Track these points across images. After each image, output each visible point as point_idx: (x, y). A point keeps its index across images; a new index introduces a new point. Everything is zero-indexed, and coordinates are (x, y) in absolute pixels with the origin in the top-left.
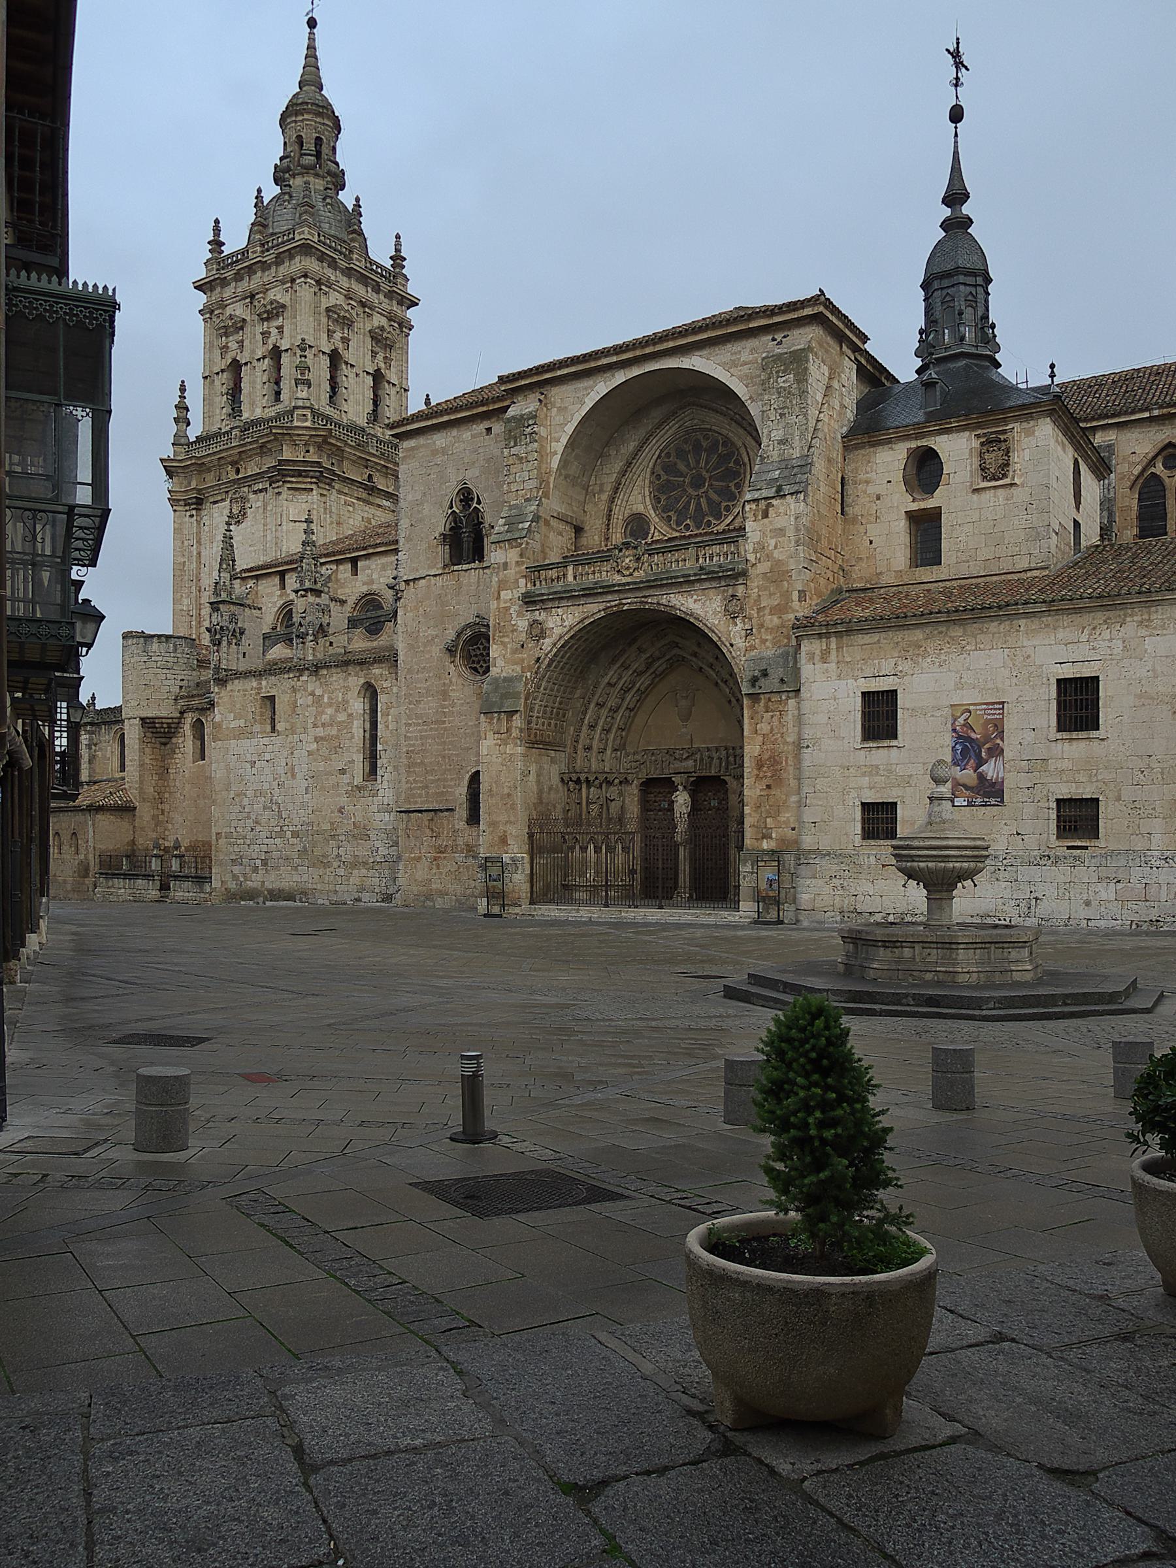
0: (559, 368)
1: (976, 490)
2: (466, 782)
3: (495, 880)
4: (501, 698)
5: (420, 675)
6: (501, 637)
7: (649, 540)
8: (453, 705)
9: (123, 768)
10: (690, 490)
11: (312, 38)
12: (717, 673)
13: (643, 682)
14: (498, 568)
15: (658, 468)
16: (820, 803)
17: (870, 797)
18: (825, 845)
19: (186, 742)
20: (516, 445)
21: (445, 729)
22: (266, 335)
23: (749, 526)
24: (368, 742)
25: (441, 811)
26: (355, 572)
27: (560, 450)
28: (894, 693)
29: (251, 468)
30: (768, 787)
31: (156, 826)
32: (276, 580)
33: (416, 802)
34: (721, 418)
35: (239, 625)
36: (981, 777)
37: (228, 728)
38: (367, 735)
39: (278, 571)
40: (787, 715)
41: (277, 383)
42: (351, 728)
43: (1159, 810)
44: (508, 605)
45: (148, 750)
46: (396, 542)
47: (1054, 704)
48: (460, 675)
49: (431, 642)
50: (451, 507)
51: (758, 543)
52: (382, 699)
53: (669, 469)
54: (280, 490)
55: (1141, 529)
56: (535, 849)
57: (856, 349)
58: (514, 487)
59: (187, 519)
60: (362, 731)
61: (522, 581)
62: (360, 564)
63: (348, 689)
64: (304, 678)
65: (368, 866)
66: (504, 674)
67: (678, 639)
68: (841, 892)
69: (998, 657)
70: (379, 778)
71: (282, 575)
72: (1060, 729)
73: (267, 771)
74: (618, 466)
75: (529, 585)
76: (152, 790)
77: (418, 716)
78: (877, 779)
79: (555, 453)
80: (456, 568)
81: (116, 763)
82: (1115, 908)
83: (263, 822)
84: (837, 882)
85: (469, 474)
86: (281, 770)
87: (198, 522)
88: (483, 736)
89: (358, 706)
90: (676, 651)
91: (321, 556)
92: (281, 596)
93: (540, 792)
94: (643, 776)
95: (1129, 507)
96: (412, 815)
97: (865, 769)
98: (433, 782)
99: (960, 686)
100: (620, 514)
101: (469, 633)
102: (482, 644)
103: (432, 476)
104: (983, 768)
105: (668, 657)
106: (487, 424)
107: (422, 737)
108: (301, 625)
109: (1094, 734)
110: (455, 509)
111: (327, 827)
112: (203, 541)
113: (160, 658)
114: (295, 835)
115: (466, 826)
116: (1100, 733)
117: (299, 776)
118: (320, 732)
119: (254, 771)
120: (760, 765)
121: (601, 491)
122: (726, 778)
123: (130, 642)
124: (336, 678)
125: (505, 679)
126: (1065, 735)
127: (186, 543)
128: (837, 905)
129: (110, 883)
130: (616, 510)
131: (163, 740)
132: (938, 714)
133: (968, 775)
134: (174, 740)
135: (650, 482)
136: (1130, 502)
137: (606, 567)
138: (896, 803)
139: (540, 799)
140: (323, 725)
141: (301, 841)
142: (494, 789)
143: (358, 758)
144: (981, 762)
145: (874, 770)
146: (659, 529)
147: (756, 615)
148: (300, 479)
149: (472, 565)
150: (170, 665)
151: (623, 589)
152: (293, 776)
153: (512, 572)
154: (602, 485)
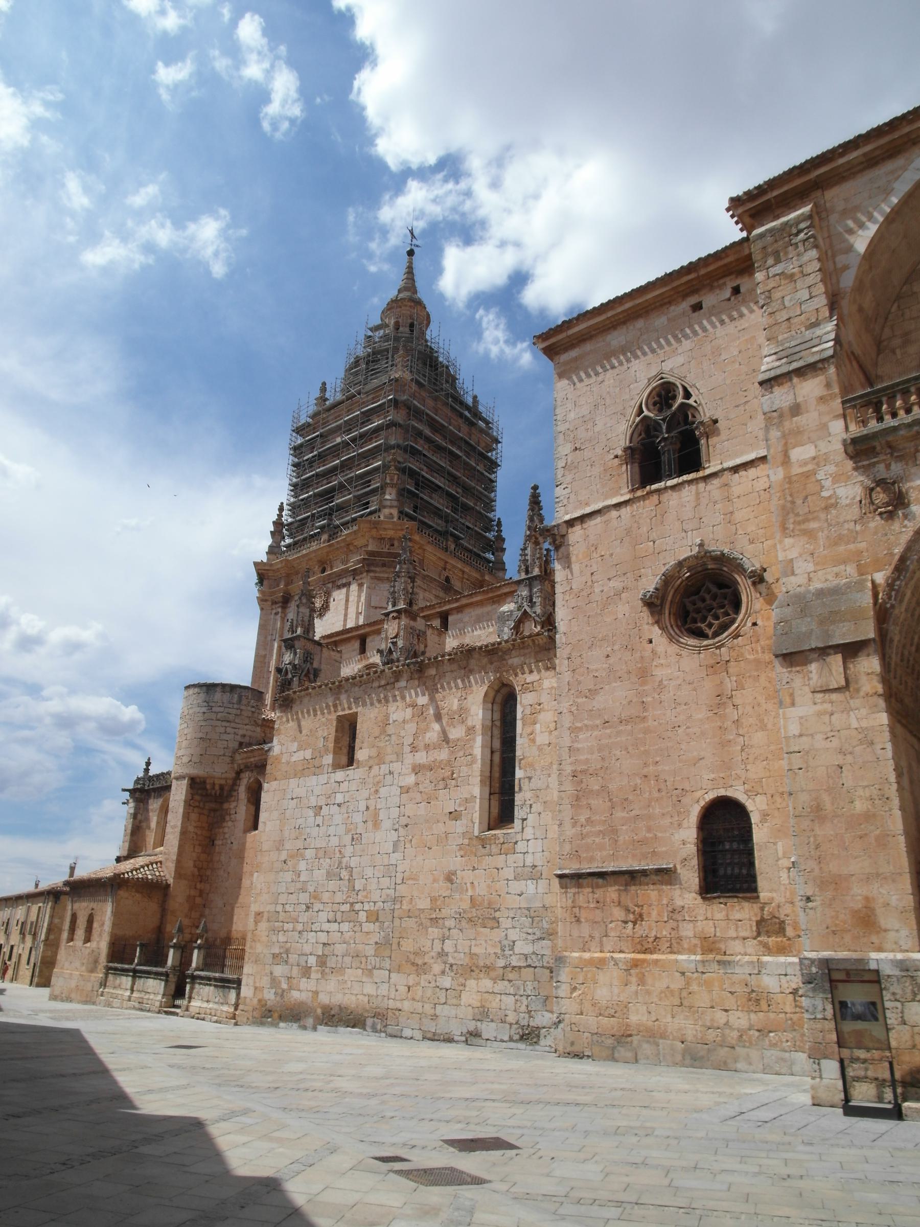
0: (842, 155)
3: (858, 1017)
4: (821, 623)
6: (799, 523)
8: (661, 686)
11: (411, 263)
14: (781, 416)
20: (778, 261)
21: (647, 731)
33: (592, 859)
35: (315, 665)
37: (288, 763)
38: (497, 758)
42: (472, 747)
44: (810, 467)
50: (641, 411)
58: (784, 315)
59: (272, 616)
61: (837, 426)
62: (450, 618)
64: (403, 683)
65: (493, 974)
66: (817, 585)
70: (517, 823)
73: (338, 819)
75: (853, 427)
79: (846, 268)
80: (654, 487)
83: (326, 897)
85: (667, 366)
86: (358, 818)
87: (283, 619)
88: (787, 700)
102: (709, 591)
103: (606, 383)
106: (693, 300)
110: (646, 413)
114: (374, 917)
115: (699, 900)
117: (387, 824)
118: (421, 757)
119: (319, 820)
125: (820, 593)
127: (269, 638)
140: (427, 747)
141: (381, 928)
142: (828, 806)
148: (384, 569)
149: (685, 477)
152: (377, 824)
153: (809, 419)
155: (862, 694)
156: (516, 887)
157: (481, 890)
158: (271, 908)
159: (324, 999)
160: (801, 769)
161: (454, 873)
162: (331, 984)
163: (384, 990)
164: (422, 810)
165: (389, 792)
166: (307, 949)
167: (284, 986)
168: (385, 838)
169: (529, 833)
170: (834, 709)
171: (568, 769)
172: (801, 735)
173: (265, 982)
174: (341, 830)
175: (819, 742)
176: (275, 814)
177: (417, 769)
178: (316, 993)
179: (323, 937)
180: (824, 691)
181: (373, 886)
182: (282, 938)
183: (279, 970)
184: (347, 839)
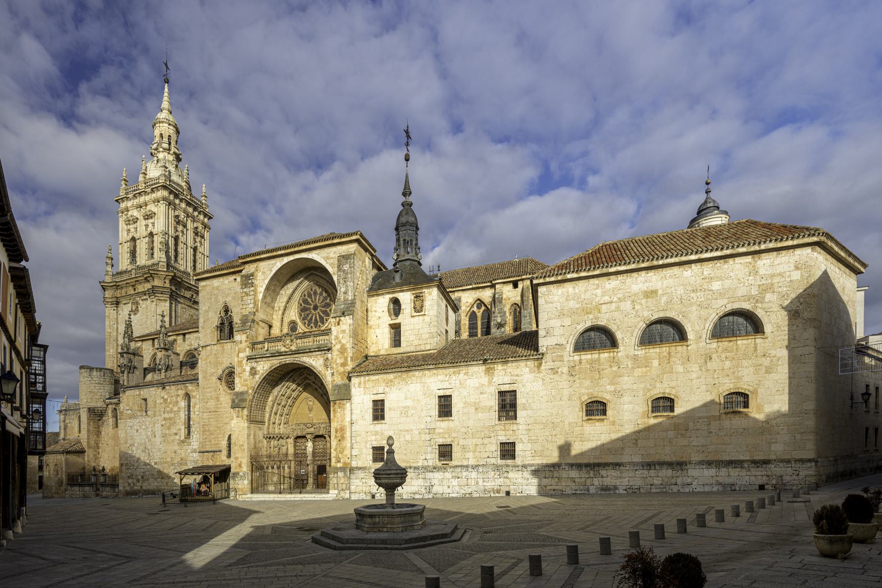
1: (412, 316)
2: (226, 439)
5: (208, 390)
7: (297, 332)
9: (80, 431)
10: (313, 311)
12: (322, 391)
15: (301, 301)
18: (360, 465)
19: (109, 420)
22: (147, 226)
23: (333, 328)
24: (187, 420)
25: (216, 452)
26: (184, 340)
27: (263, 291)
28: (383, 401)
29: (141, 288)
30: (340, 440)
31: (96, 459)
32: (151, 342)
34: (324, 280)
38: (187, 417)
39: (151, 337)
41: (152, 249)
43: (471, 449)
45: (92, 423)
46: (198, 327)
47: (437, 406)
48: (224, 390)
49: (212, 375)
52: (193, 400)
53: (305, 301)
54: (153, 300)
55: (470, 333)
57: (372, 255)
60: (184, 415)
63: (178, 395)
69: (418, 387)
71: (153, 339)
72: (440, 416)
73: (144, 434)
74: (285, 299)
76: (93, 442)
77: (207, 409)
78: (378, 437)
81: (77, 429)
82: (457, 488)
84: (364, 480)
86: (149, 433)
89: (183, 404)
91: (170, 332)
92: (153, 350)
93: (255, 443)
95: (465, 324)
96: (205, 454)
98: (213, 438)
99: (406, 398)
100: (287, 320)
101: (227, 371)
107: (209, 418)
108: (159, 364)
109: (450, 418)
111: (169, 460)
112: (119, 322)
113: (97, 379)
116: (452, 418)
117: (158, 436)
118: (166, 416)
120: (336, 431)
121: (279, 310)
123: (83, 371)
124: (172, 390)
126: (441, 419)
128: (364, 490)
129: (73, 489)
130: (285, 319)
131: (98, 418)
132: (398, 410)
134: (104, 418)
135: (298, 307)
136: (465, 321)
137: (281, 343)
139: (255, 447)
143: (183, 427)
145: (376, 433)
146: (301, 328)
150: (102, 382)
151: (285, 354)
152: (155, 436)
154: (279, 307)
156: (191, 454)
157: (183, 456)
158: (126, 462)
159: (144, 488)
161: (176, 451)
162: (146, 484)
163: (160, 484)
164: (167, 432)
165: (158, 426)
166: (138, 474)
167: (132, 485)
168: (158, 439)
169: (194, 440)
171: (201, 424)
173: (126, 484)
174: (145, 437)
176: (124, 431)
177: (165, 419)
178: (141, 487)
179: (142, 470)
181: (155, 454)
182: (130, 471)
183: (130, 481)
184: (147, 440)
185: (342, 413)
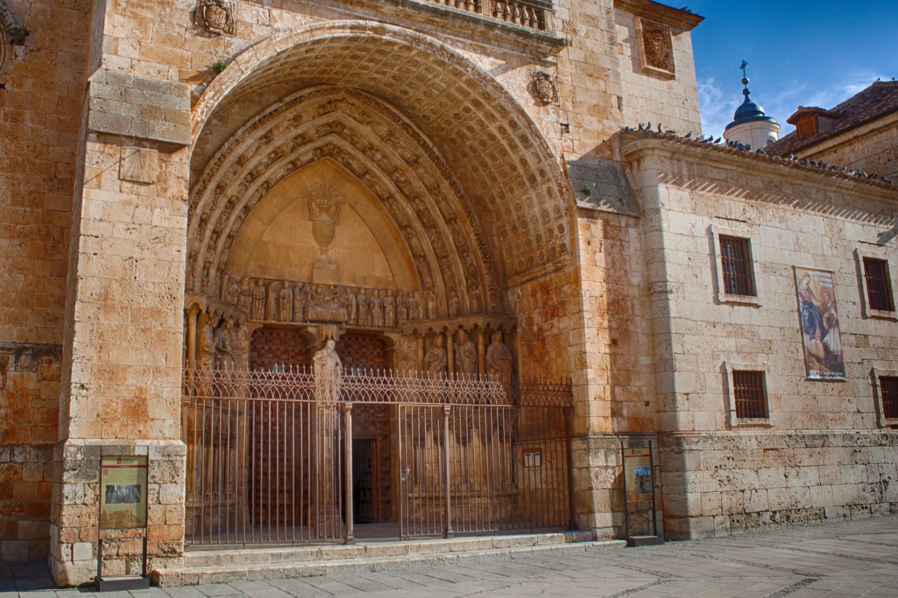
13: (277, 170)
16: (690, 368)
17: (742, 365)
36: (826, 347)
40: (629, 247)
51: (569, 24)
56: (189, 437)
67: (350, 122)
68: (727, 488)
84: (723, 473)
90: (333, 139)
94: (259, 323)
97: (730, 329)
104: (827, 338)
105: (319, 144)
122: (394, 336)
128: (726, 507)
133: (814, 345)
138: (764, 372)
144: (824, 333)
147: (571, 109)
155: (169, 194)
160: (95, 254)
170: (140, 202)
172: (101, 220)
175: (120, 231)
180: (133, 182)
185: (617, 256)
